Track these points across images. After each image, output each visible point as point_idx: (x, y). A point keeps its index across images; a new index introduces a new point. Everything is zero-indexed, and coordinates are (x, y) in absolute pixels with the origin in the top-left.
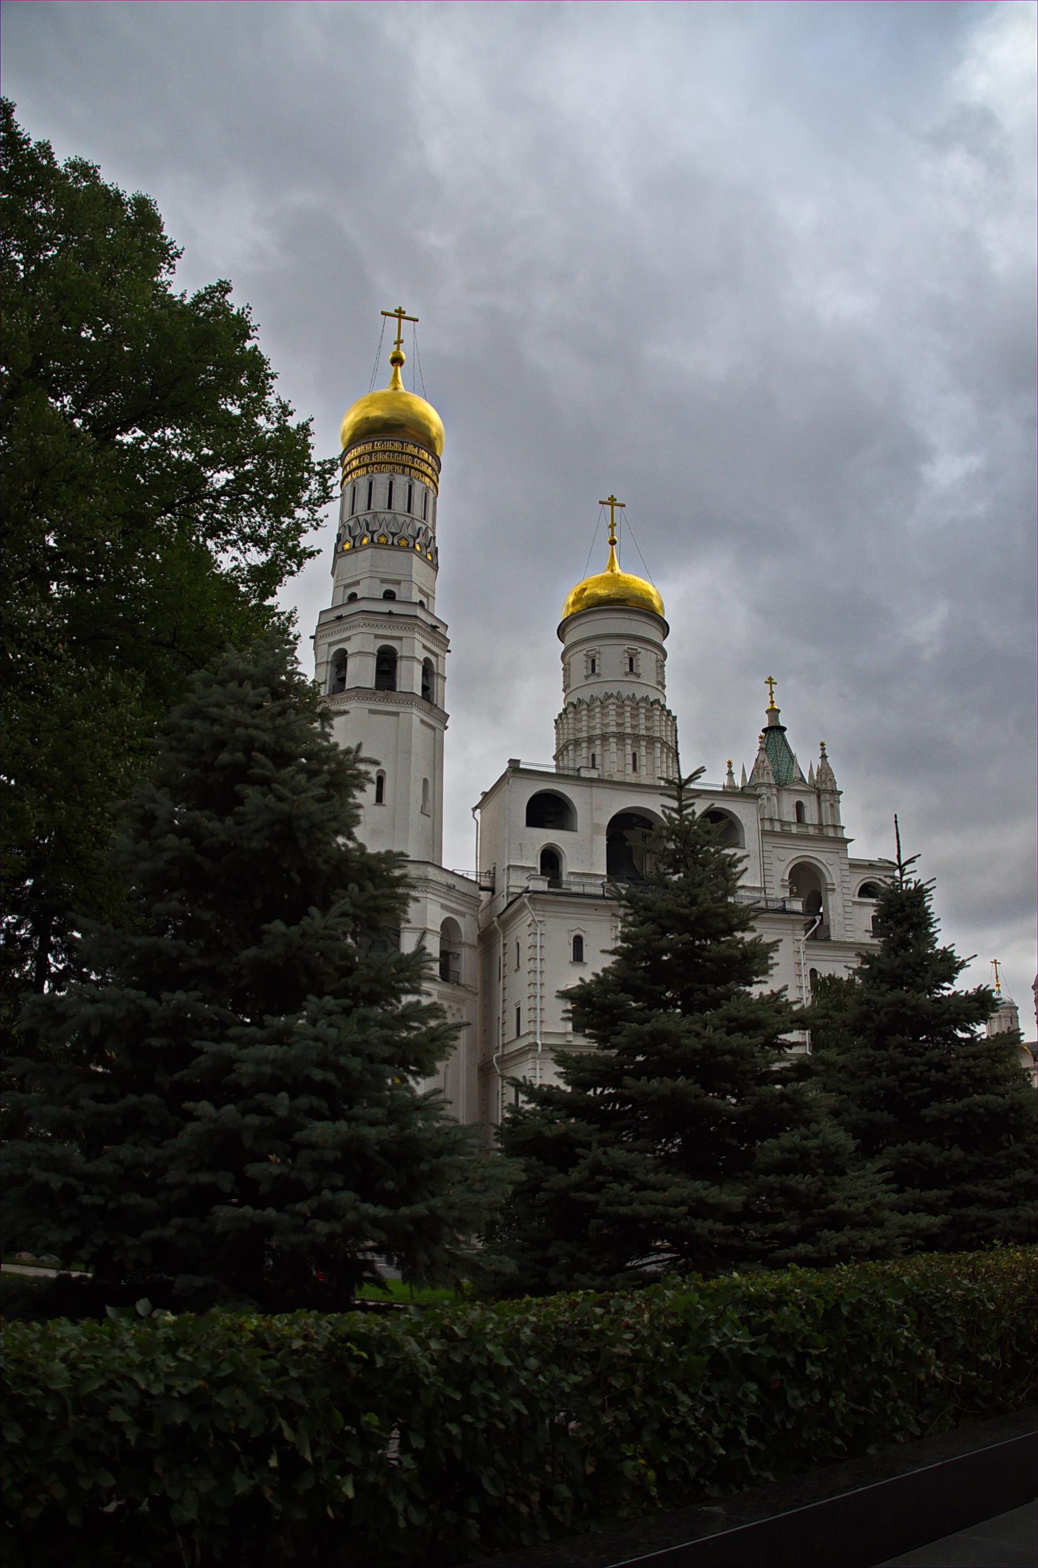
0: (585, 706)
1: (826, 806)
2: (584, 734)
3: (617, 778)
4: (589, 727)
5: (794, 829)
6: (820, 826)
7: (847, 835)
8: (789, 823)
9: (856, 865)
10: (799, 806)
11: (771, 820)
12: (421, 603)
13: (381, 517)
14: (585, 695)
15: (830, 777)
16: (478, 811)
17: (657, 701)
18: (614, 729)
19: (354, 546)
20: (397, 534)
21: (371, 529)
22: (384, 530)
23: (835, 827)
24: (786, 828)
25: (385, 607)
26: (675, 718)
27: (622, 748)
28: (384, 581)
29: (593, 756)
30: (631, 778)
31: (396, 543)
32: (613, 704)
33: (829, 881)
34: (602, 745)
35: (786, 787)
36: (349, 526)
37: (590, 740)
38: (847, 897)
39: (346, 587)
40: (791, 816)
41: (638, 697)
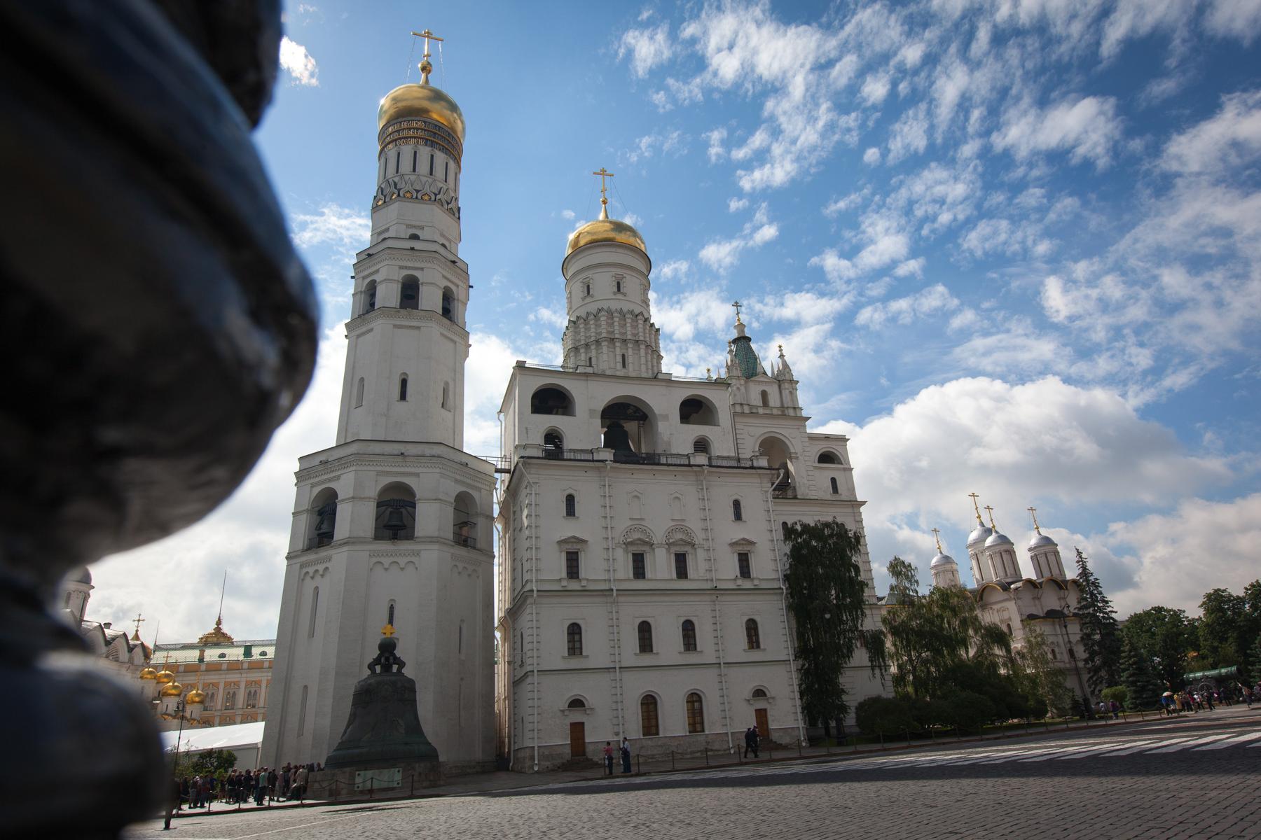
0: (582, 321)
1: (786, 393)
2: (583, 342)
3: (608, 373)
4: (586, 337)
5: (761, 411)
6: (782, 407)
7: (804, 414)
8: (757, 407)
9: (814, 438)
10: (764, 395)
11: (741, 404)
12: (443, 245)
13: (407, 178)
14: (582, 312)
15: (787, 370)
16: (502, 414)
17: (641, 313)
18: (604, 335)
19: (385, 202)
21: (398, 188)
22: (408, 187)
23: (795, 408)
24: (754, 411)
26: (658, 330)
27: (613, 350)
28: (408, 226)
29: (590, 359)
30: (621, 373)
31: (419, 197)
32: (604, 316)
33: (792, 450)
34: (597, 350)
35: (752, 379)
36: (382, 188)
37: (587, 345)
38: (809, 463)
39: (379, 234)
40: (756, 400)
41: (625, 310)
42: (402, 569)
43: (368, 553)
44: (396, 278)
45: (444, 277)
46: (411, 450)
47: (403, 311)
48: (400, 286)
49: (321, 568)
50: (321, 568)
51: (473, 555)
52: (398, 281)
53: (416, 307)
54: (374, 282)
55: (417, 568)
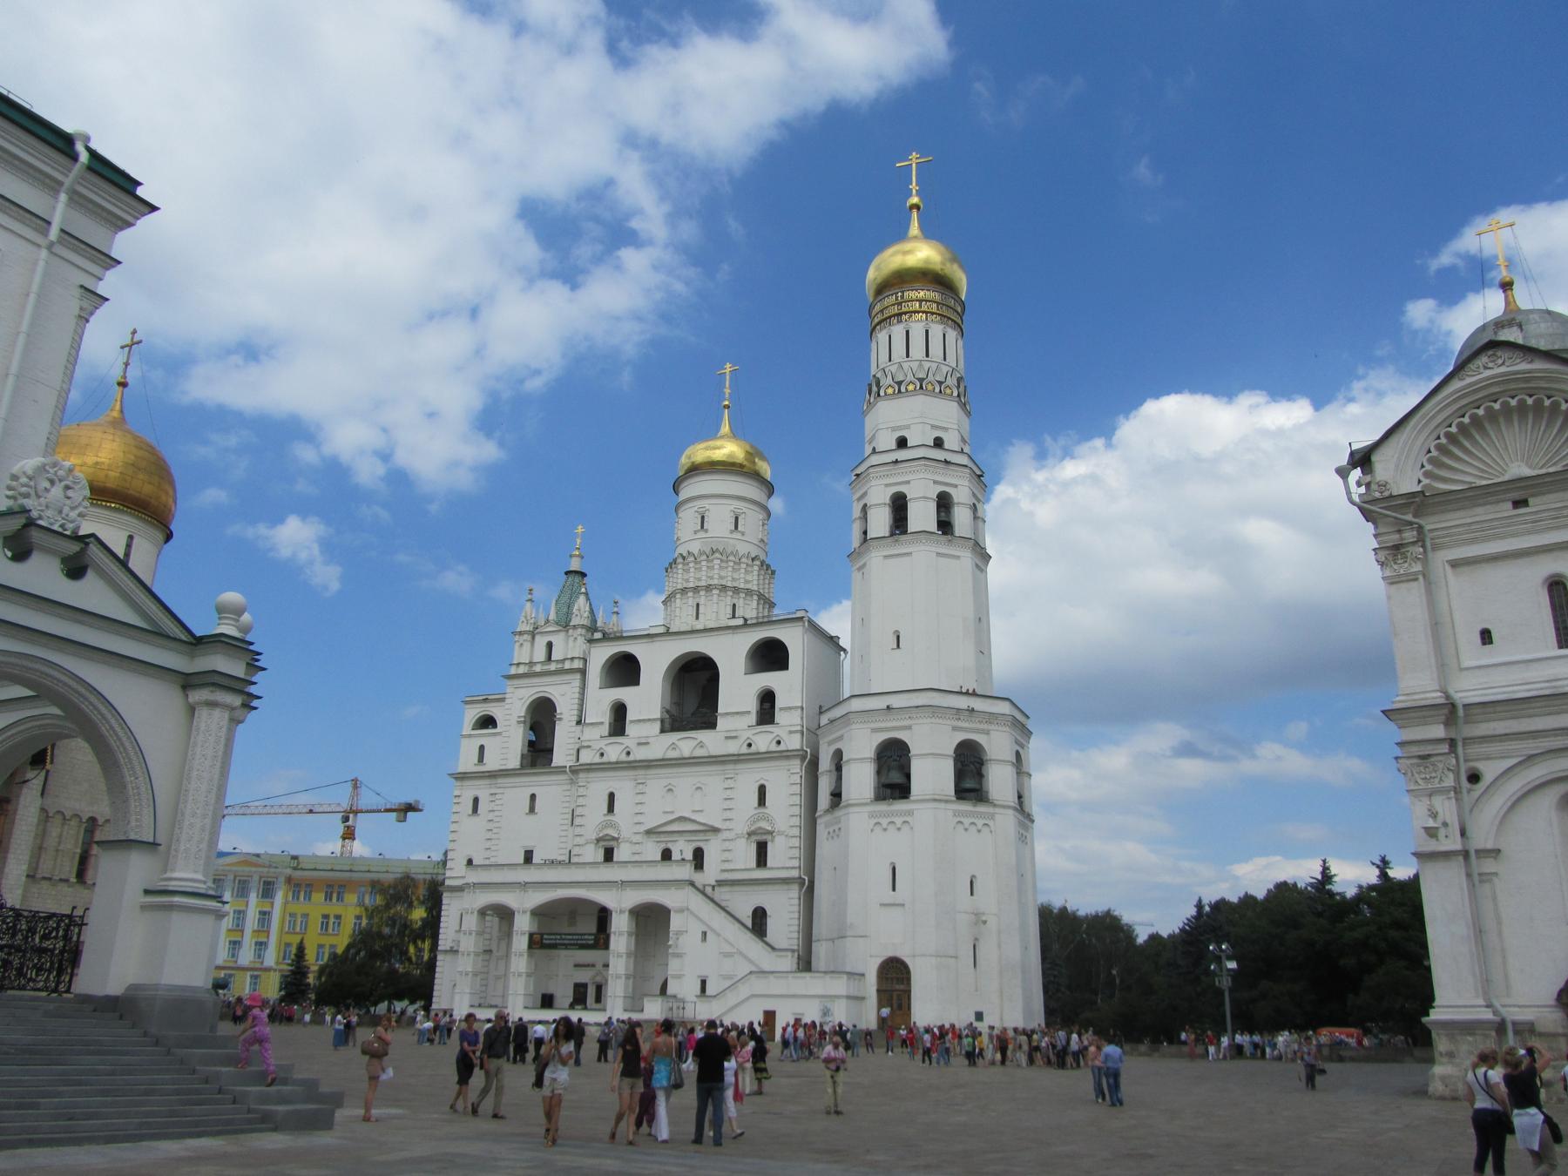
20: (903, 381)
25: (903, 455)
28: (894, 429)
31: (903, 390)
42: (899, 829)
43: (866, 815)
44: (883, 502)
45: (935, 482)
46: (896, 702)
47: (892, 538)
48: (887, 506)
49: (836, 828)
50: (836, 828)
51: (982, 808)
52: (885, 504)
53: (904, 532)
54: (865, 505)
55: (912, 828)
